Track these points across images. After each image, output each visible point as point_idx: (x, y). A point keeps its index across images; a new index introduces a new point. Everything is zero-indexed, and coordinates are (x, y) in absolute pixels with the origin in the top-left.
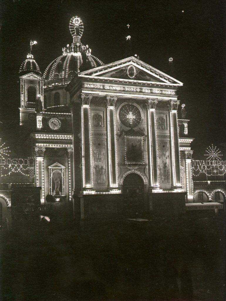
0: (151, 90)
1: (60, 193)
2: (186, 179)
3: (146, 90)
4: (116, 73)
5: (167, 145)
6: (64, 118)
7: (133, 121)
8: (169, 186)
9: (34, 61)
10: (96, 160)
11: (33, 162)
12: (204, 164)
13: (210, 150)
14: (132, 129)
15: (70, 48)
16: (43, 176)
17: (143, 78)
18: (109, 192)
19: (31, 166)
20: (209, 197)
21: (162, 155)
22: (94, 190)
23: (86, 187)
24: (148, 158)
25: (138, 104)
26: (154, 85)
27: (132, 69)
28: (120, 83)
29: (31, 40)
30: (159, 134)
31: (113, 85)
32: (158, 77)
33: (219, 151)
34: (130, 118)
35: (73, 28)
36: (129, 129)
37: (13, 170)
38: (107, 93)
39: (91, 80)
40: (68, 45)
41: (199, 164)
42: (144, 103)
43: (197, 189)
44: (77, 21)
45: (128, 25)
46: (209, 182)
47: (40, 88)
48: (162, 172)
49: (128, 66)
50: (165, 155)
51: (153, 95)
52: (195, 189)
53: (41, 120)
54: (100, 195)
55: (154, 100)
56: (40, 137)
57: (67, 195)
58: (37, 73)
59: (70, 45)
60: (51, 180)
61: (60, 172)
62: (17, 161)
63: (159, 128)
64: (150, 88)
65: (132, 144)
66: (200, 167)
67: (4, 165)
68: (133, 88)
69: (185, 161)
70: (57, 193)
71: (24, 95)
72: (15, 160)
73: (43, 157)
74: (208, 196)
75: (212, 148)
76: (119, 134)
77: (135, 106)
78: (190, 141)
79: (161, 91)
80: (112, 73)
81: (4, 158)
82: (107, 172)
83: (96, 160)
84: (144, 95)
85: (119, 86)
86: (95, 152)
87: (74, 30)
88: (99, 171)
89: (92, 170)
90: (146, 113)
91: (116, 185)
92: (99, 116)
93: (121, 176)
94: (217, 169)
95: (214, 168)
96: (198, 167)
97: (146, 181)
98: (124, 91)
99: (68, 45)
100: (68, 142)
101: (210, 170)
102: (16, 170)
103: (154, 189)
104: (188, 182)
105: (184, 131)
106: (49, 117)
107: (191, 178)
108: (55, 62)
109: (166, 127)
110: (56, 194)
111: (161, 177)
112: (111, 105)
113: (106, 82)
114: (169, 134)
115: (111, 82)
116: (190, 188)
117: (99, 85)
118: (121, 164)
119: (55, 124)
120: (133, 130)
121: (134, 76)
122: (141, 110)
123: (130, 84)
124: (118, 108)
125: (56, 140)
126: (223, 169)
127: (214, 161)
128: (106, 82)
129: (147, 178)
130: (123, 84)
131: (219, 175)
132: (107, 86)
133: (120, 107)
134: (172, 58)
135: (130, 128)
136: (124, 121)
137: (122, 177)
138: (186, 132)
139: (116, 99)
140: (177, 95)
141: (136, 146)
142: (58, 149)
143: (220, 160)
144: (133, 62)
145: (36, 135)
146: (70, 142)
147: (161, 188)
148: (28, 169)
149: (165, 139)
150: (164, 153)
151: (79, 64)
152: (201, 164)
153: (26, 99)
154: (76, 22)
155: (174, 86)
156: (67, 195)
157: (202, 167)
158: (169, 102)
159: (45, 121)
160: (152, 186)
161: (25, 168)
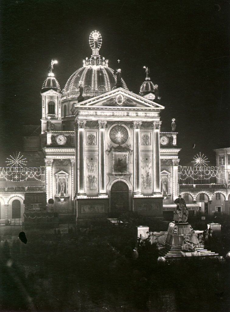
0: (136, 113)
1: (65, 194)
2: (173, 183)
3: (132, 114)
4: (107, 101)
5: (150, 158)
6: (69, 135)
7: (121, 138)
8: (150, 191)
9: (55, 78)
10: (89, 171)
11: (44, 170)
12: (191, 170)
14: (120, 145)
15: (88, 61)
16: (51, 181)
17: (129, 104)
18: (98, 196)
19: (43, 173)
20: (194, 198)
21: (146, 166)
22: (86, 195)
23: (80, 193)
24: (131, 169)
25: (126, 125)
26: (139, 109)
27: (120, 98)
28: (110, 109)
29: (52, 60)
30: (143, 149)
31: (104, 111)
32: (143, 102)
33: (206, 158)
34: (119, 137)
35: (93, 42)
36: (116, 145)
37: (29, 176)
38: (99, 118)
39: (85, 109)
40: (87, 59)
41: (186, 170)
42: (131, 124)
43: (183, 191)
44: (95, 35)
45: (119, 61)
46: (194, 185)
47: (59, 102)
48: (145, 179)
49: (117, 95)
50: (148, 166)
51: (138, 118)
52: (180, 191)
53: (50, 137)
54: (91, 199)
55: (139, 122)
56: (49, 151)
57: (70, 196)
58: (56, 90)
59: (89, 59)
60: (58, 184)
61: (64, 177)
62: (32, 170)
63: (144, 144)
64: (136, 112)
65: (119, 158)
66: (187, 172)
67: (22, 173)
68: (121, 113)
69: (173, 167)
70: (62, 195)
71: (45, 109)
72: (31, 169)
73: (51, 167)
74: (192, 197)
76: (109, 150)
77: (123, 127)
78: (178, 150)
79: (145, 113)
81: (22, 167)
82: (98, 181)
83: (89, 171)
84: (131, 118)
85: (109, 111)
86: (89, 165)
87: (93, 44)
88: (91, 180)
89: (86, 179)
90: (132, 132)
91: (104, 191)
92: (93, 136)
93: (109, 183)
94: (203, 173)
95: (200, 173)
96: (185, 172)
97: (130, 188)
98: (113, 115)
99: (87, 59)
101: (197, 175)
102: (31, 176)
103: (135, 194)
104: (174, 186)
105: (172, 142)
106: (57, 135)
107: (177, 182)
108: (74, 75)
109: (150, 143)
110: (61, 196)
111: (144, 184)
112: (102, 128)
113: (98, 109)
114: (152, 149)
115: (102, 109)
116: (176, 190)
117: (92, 112)
118: (110, 174)
119: (61, 140)
120: (122, 147)
121: (122, 103)
122: (128, 130)
123: (118, 110)
124: (109, 129)
125: (62, 153)
126: (209, 174)
127: (200, 167)
128: (98, 109)
129: (132, 184)
130: (113, 110)
131: (205, 179)
132: (99, 113)
133: (111, 128)
134: (157, 85)
135: (118, 145)
136: (113, 140)
137: (111, 184)
138: (175, 143)
139: (106, 123)
140: (160, 116)
141: (122, 160)
142: (63, 160)
143: (206, 166)
144: (121, 91)
145: (46, 149)
146: (73, 154)
147: (142, 194)
148: (40, 175)
149: (148, 153)
150: (147, 164)
151: (93, 79)
152: (188, 170)
153: (47, 112)
154: (96, 36)
155: (158, 110)
156: (70, 196)
157: (189, 172)
158: (152, 123)
159: (53, 138)
160: (135, 192)
161: (38, 175)
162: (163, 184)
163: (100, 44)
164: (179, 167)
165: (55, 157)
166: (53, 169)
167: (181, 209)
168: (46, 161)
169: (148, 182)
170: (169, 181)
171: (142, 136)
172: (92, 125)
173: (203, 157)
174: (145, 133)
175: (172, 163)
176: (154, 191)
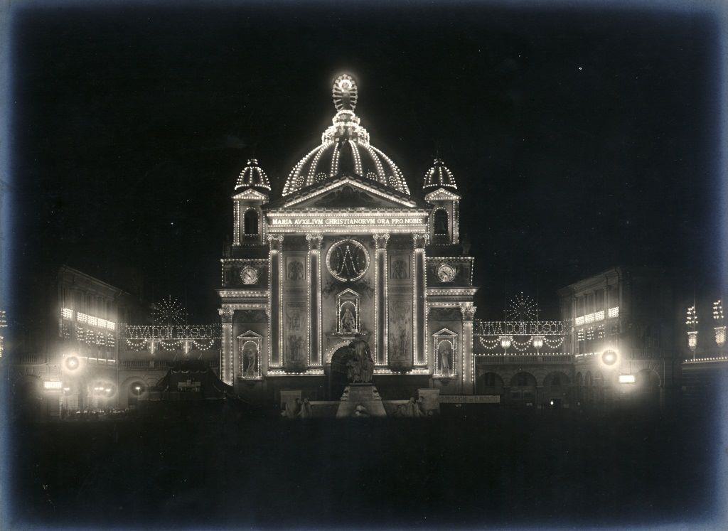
11: (219, 331)
13: (530, 305)
44: (345, 84)
48: (397, 344)
50: (403, 318)
75: (520, 299)
80: (317, 199)
86: (290, 316)
88: (295, 344)
92: (298, 264)
100: (264, 301)
139: (321, 238)
145: (221, 293)
150: (402, 315)
162: (443, 354)
163: (354, 99)
164: (476, 327)
166: (235, 328)
167: (358, 358)
168: (221, 312)
169: (401, 347)
170: (453, 348)
172: (295, 243)
174: (399, 257)
176: (415, 364)
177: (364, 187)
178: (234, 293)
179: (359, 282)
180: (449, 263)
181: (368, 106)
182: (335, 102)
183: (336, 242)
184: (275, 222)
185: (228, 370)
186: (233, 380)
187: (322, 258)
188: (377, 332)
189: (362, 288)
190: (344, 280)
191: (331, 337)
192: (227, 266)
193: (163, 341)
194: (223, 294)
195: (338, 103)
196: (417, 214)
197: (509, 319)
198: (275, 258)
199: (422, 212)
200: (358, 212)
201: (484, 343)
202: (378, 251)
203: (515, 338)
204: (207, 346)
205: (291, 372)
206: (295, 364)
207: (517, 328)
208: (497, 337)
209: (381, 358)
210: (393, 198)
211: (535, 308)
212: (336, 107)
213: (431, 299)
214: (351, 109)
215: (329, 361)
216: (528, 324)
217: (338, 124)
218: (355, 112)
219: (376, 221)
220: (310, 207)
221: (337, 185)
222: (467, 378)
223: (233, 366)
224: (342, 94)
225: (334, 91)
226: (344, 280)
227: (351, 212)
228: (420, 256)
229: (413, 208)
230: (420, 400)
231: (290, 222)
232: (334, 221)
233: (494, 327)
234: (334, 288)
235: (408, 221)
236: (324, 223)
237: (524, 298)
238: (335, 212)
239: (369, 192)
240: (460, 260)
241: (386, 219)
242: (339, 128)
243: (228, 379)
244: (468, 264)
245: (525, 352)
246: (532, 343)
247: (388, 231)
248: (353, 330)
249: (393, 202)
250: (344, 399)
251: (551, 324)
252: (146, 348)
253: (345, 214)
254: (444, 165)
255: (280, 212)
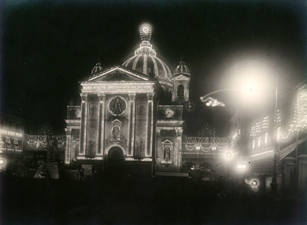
11: (65, 138)
44: (146, 29)
75: (206, 127)
80: (103, 77)
83: (91, 137)
88: (91, 145)
92: (95, 107)
97: (124, 154)
163: (150, 36)
165: (74, 127)
168: (66, 130)
171: (138, 107)
172: (93, 98)
173: (210, 128)
175: (176, 133)
177: (125, 71)
178: (72, 121)
179: (122, 116)
180: (171, 109)
181: (155, 38)
182: (141, 37)
183: (112, 97)
184: (84, 88)
185: (68, 156)
186: (70, 161)
187: (104, 106)
188: (128, 140)
189: (123, 119)
190: (115, 115)
191: (107, 142)
192: (70, 109)
193: (42, 142)
194: (67, 121)
195: (142, 38)
196: (149, 83)
197: (200, 136)
198: (84, 104)
199: (152, 82)
200: (121, 83)
201: (188, 147)
202: (131, 101)
203: (203, 145)
204: (61, 145)
205: (88, 157)
206: (90, 154)
207: (204, 141)
208: (194, 145)
209: (130, 153)
210: (138, 76)
211: (213, 131)
212: (142, 39)
213: (160, 125)
214: (148, 40)
215: (107, 153)
216: (210, 139)
217: (143, 47)
218: (150, 42)
219: (130, 87)
220: (100, 81)
221: (113, 70)
222: (178, 163)
223: (70, 155)
224: (145, 34)
225: (141, 32)
226: (115, 115)
227: (118, 83)
228: (150, 104)
229: (148, 81)
230: (81, 170)
231: (91, 88)
232: (111, 87)
233: (193, 140)
234: (110, 118)
235: (145, 87)
236: (106, 88)
237: (208, 127)
238: (111, 83)
239: (127, 73)
240: (177, 107)
241: (135, 86)
242: (144, 49)
243: (68, 160)
244: (181, 109)
245: (207, 152)
246: (211, 148)
247: (135, 92)
248: (118, 139)
249: (139, 78)
250: (40, 168)
251: (221, 139)
252: (35, 145)
253: (115, 84)
254: (185, 64)
255: (86, 83)
